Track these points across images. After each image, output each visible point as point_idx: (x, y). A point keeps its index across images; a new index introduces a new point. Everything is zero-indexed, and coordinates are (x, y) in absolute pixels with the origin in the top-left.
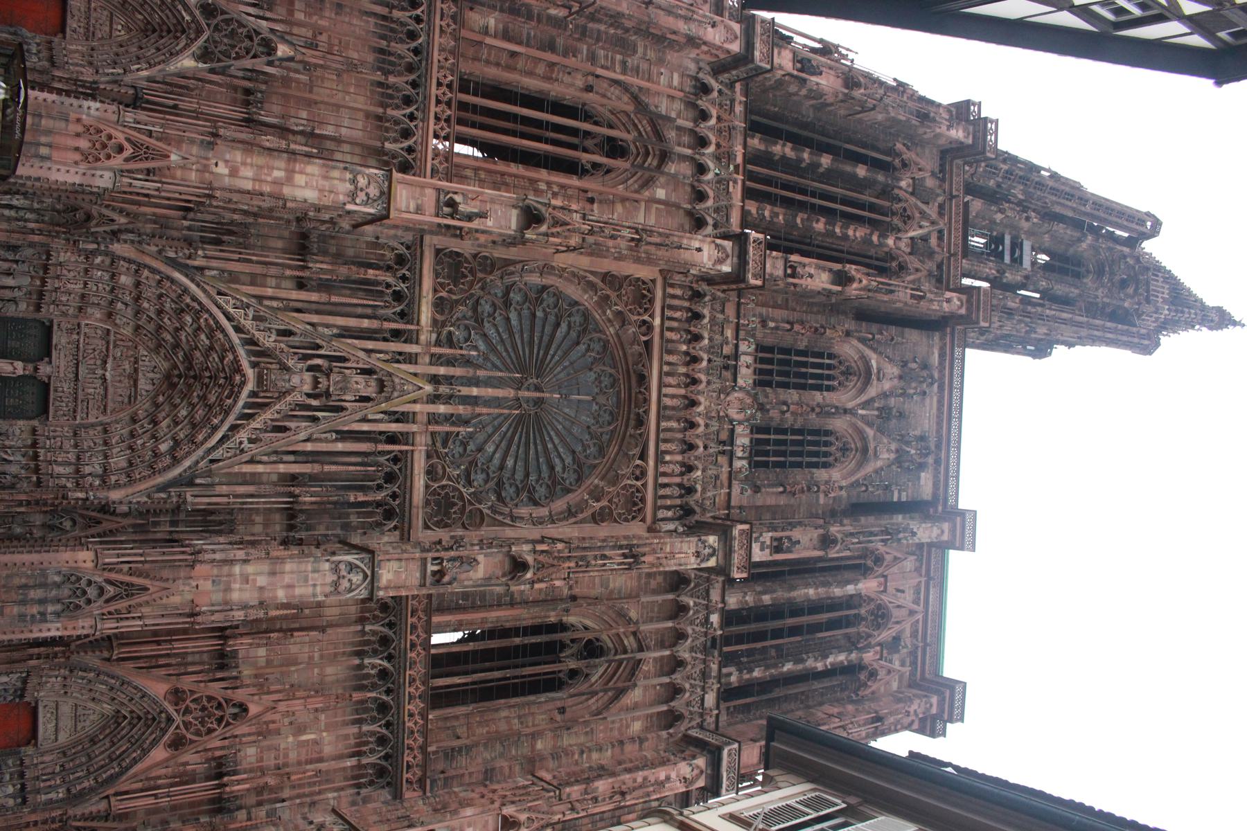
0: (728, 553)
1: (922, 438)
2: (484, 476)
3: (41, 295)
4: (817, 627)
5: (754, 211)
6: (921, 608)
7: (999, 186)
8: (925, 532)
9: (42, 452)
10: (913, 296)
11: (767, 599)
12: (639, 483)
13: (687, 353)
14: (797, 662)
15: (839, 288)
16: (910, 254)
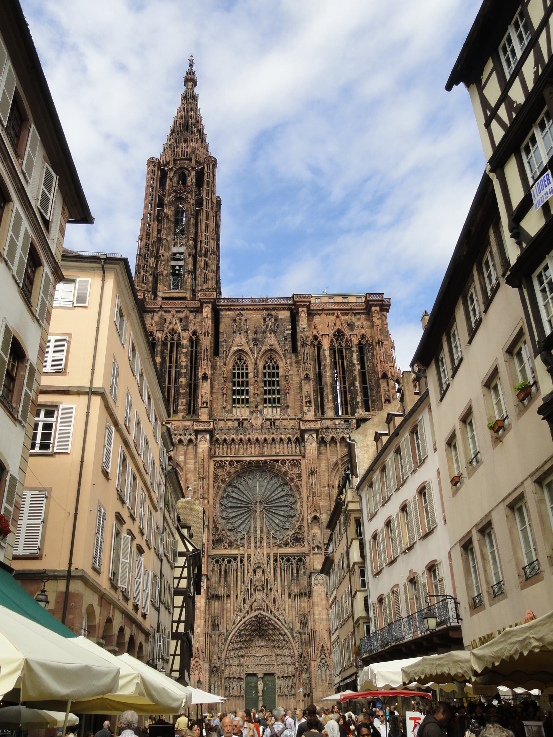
0: (311, 430)
1: (265, 320)
2: (287, 523)
3: (238, 678)
4: (343, 367)
5: (182, 414)
6: (336, 312)
7: (151, 275)
8: (303, 322)
9: (285, 675)
10: (208, 336)
11: (330, 397)
12: (287, 462)
13: (239, 444)
14: (354, 379)
15: (209, 380)
16: (188, 330)
